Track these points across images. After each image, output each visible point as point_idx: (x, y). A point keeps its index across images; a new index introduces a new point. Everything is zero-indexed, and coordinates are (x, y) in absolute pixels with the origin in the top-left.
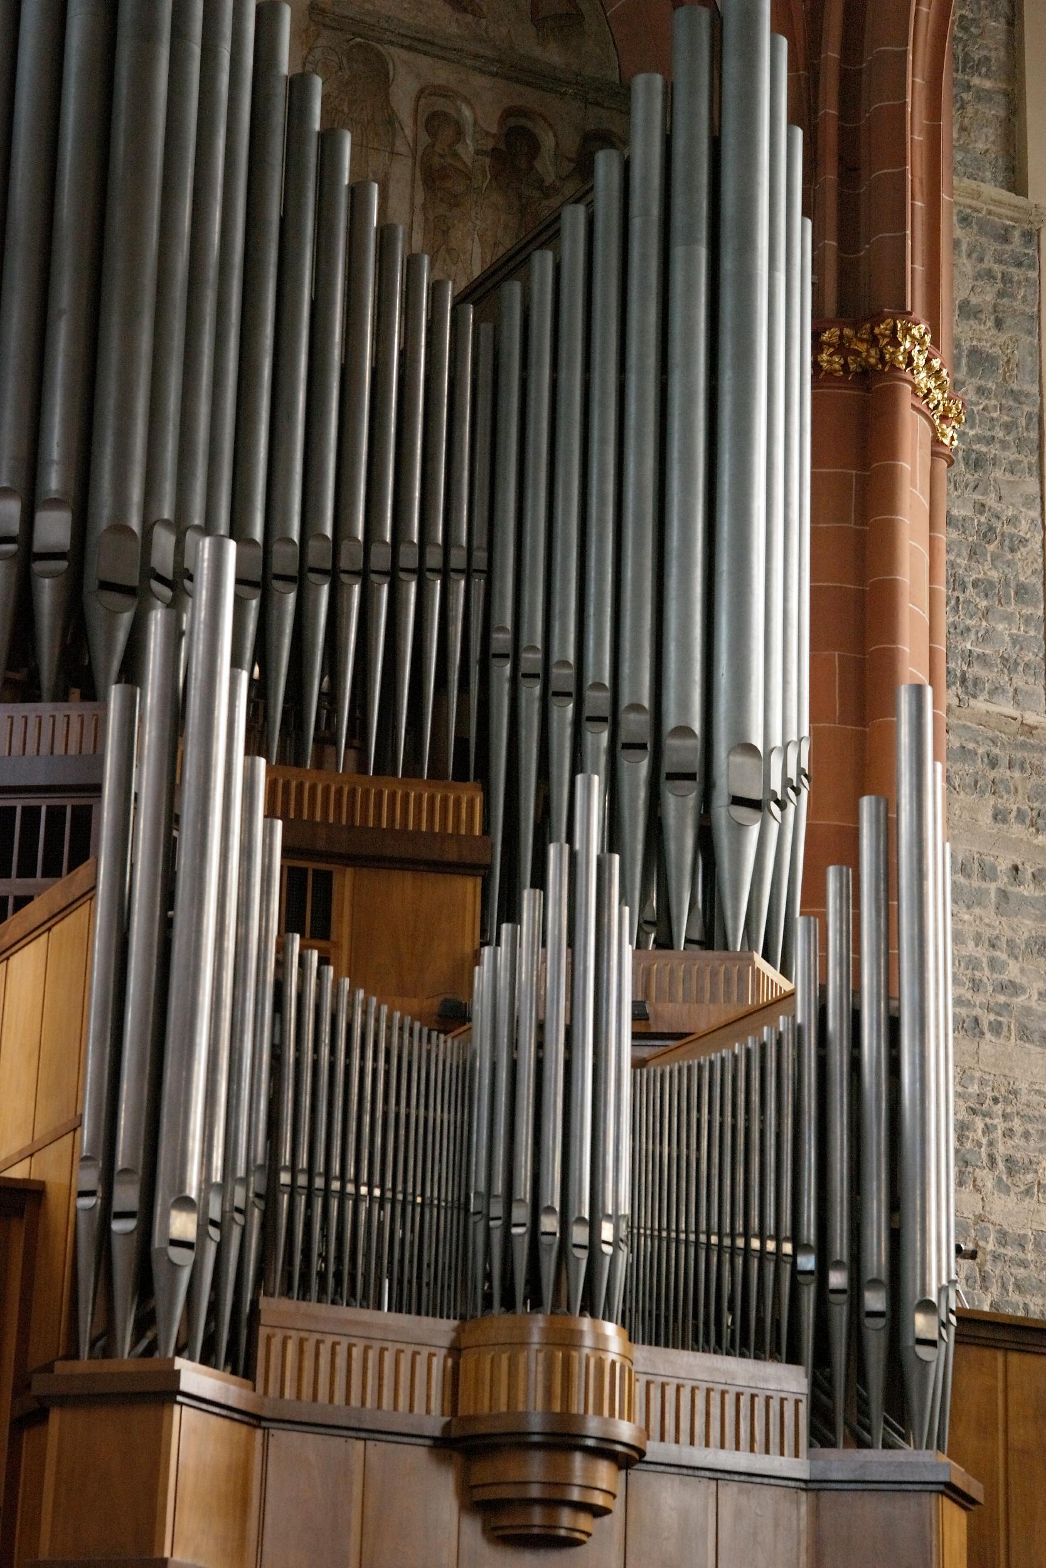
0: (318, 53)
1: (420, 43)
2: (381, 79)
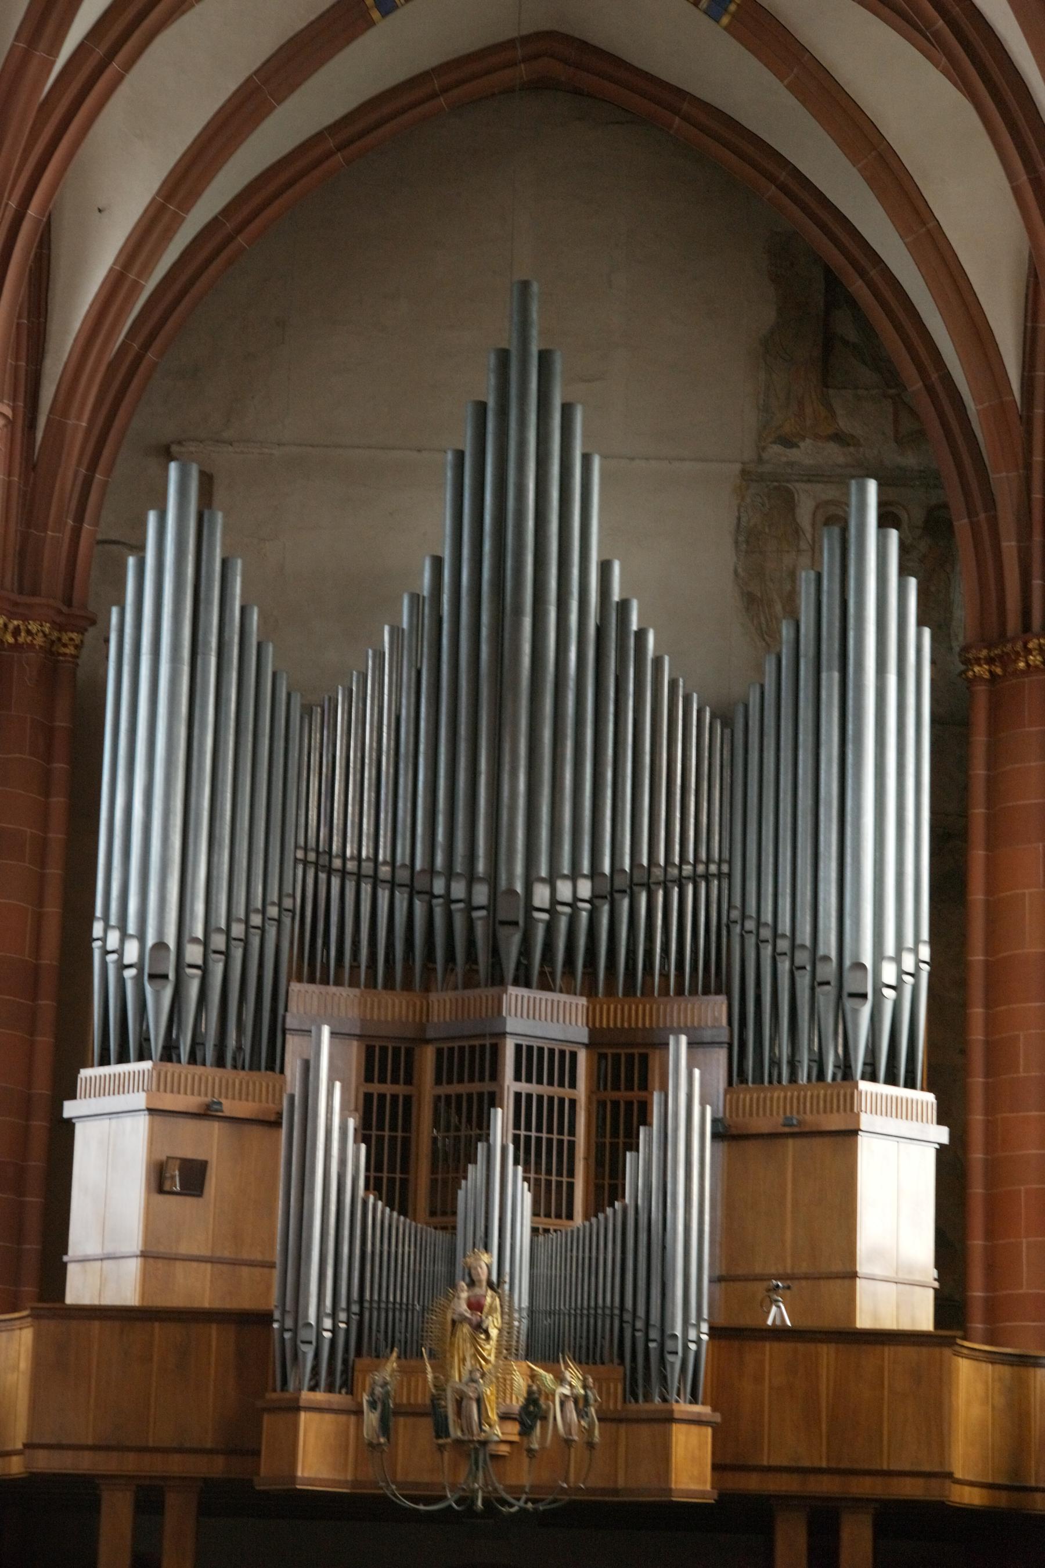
0: (748, 500)
1: (813, 476)
2: (790, 503)
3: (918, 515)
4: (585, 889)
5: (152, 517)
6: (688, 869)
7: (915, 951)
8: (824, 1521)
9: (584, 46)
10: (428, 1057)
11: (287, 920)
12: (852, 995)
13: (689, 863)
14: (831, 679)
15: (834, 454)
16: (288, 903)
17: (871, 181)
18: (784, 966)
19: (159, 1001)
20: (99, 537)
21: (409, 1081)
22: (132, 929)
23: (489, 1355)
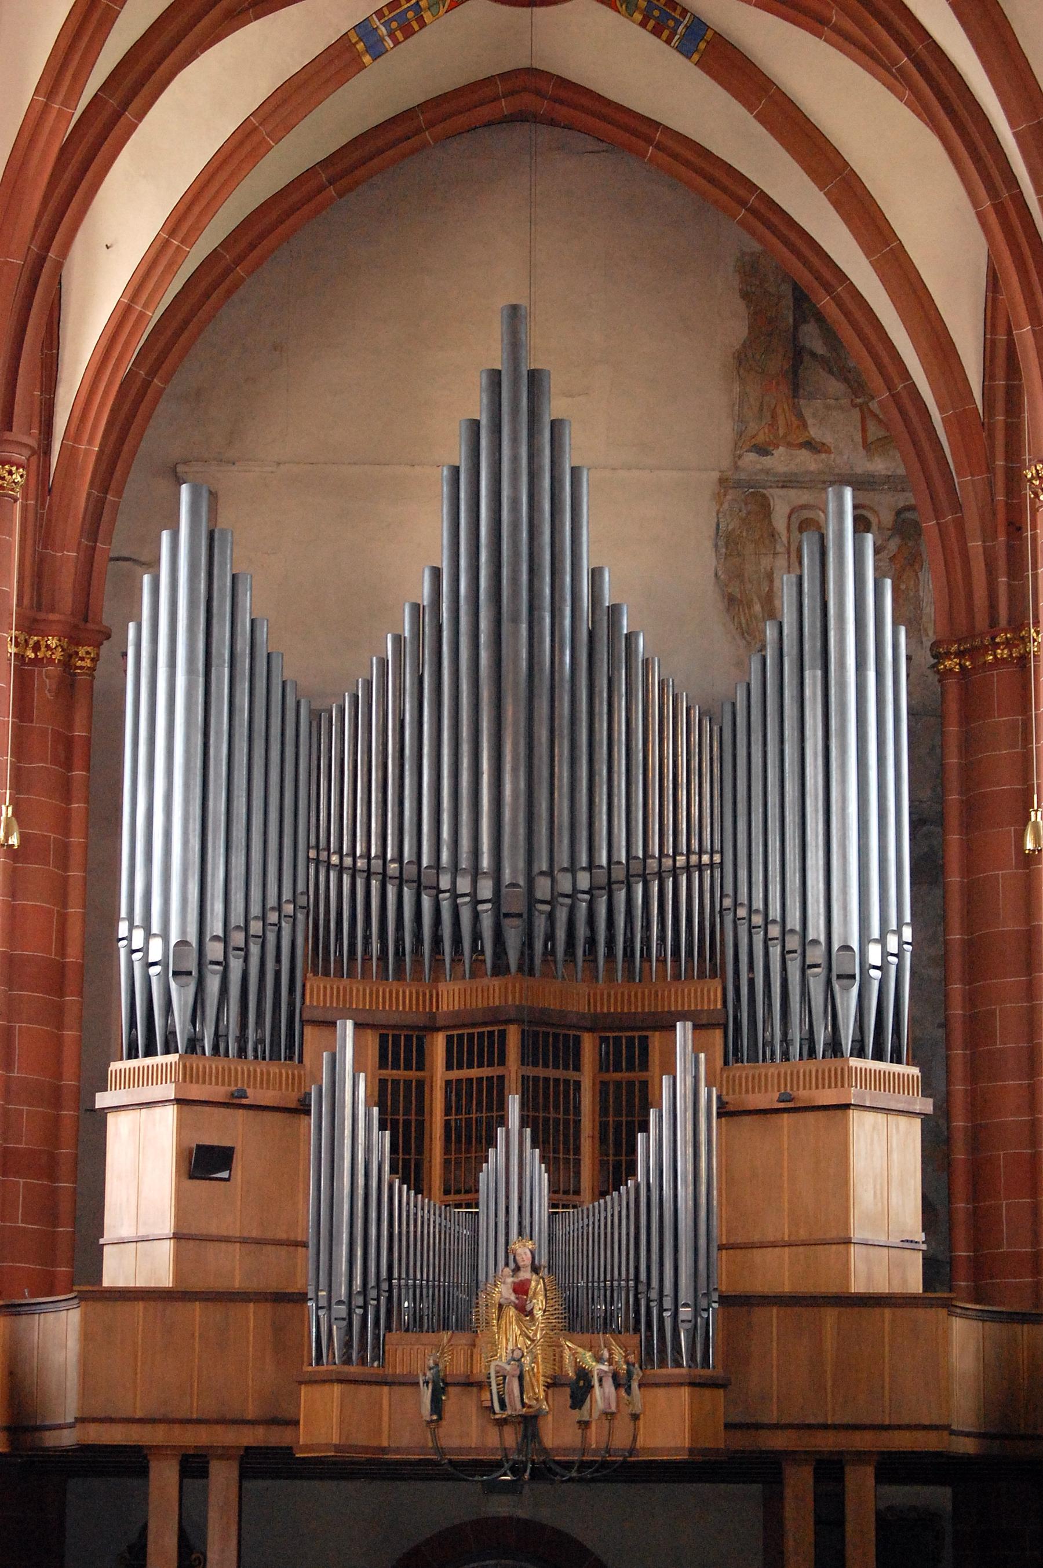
0: (726, 506)
1: (788, 482)
2: (765, 509)
3: (887, 518)
4: (584, 881)
5: (165, 536)
6: (681, 860)
7: (899, 932)
8: (830, 1470)
9: (563, 82)
10: (438, 1044)
11: (300, 917)
12: (839, 977)
13: (682, 854)
14: (812, 678)
15: (807, 462)
16: (302, 901)
17: (837, 205)
18: (775, 951)
19: (181, 996)
20: (111, 555)
21: (421, 1067)
22: (155, 928)
23: (535, 1334)
